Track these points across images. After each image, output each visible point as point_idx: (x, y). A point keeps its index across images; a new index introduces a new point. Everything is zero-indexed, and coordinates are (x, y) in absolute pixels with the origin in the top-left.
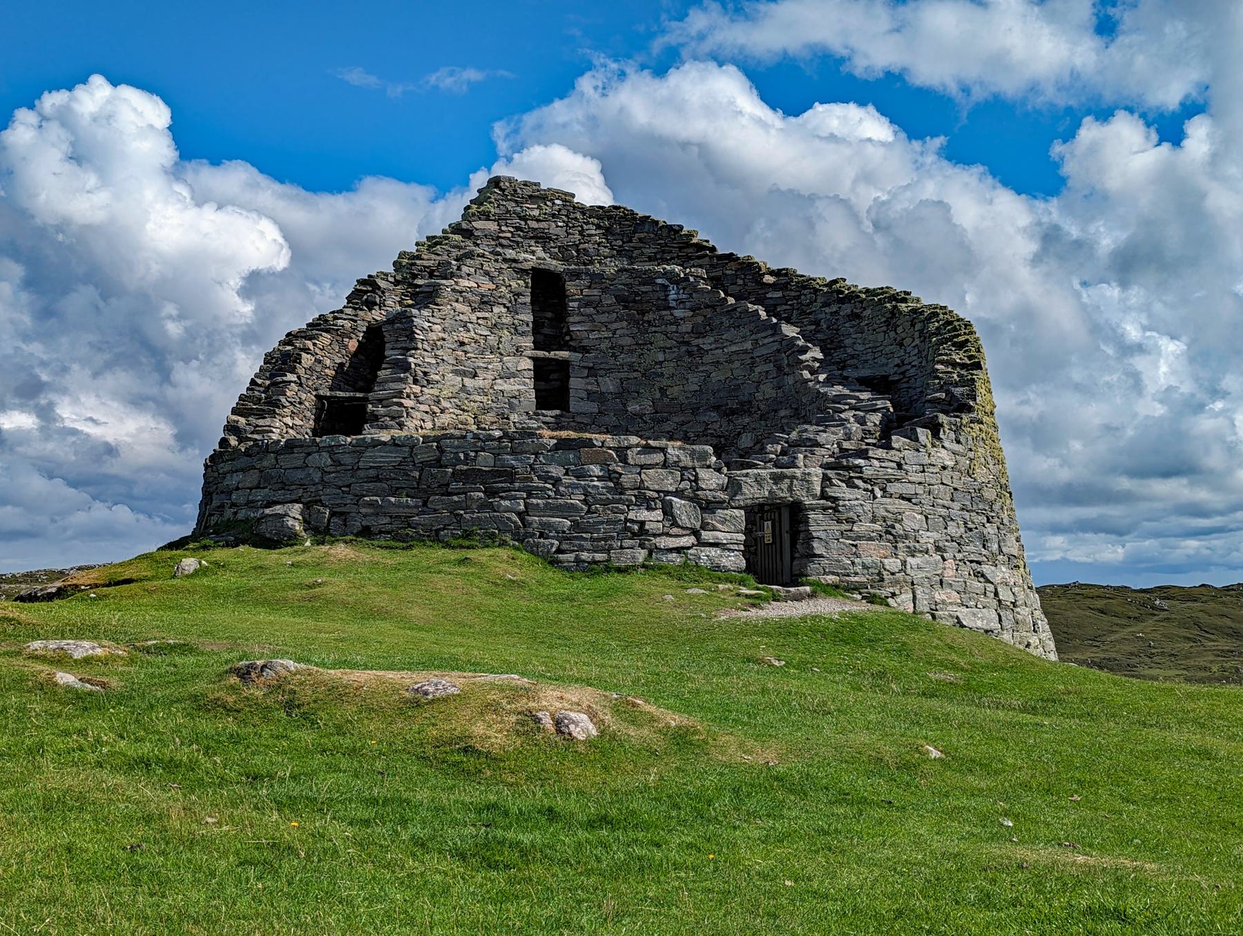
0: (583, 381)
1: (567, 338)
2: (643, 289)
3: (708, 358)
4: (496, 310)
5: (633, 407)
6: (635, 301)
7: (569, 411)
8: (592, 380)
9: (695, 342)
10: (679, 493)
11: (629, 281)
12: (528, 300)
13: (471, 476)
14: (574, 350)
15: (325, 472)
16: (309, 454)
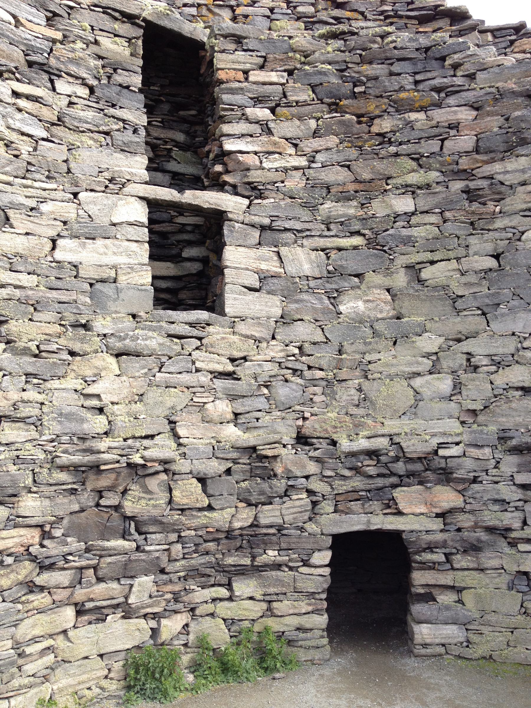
0: (252, 253)
1: (218, 168)
2: (368, 70)
4: (62, 86)
6: (354, 96)
7: (223, 313)
8: (266, 251)
9: (487, 170)
11: (341, 56)
12: (137, 80)
14: (235, 191)
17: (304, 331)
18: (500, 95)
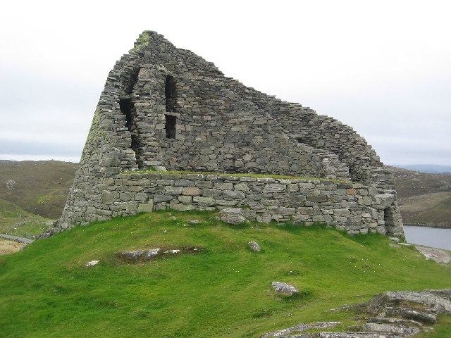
3: (231, 121)
5: (198, 139)
10: (371, 206)
13: (314, 199)
14: (178, 112)
15: (246, 193)
16: (234, 184)
17: (190, 144)
18: (230, 100)
